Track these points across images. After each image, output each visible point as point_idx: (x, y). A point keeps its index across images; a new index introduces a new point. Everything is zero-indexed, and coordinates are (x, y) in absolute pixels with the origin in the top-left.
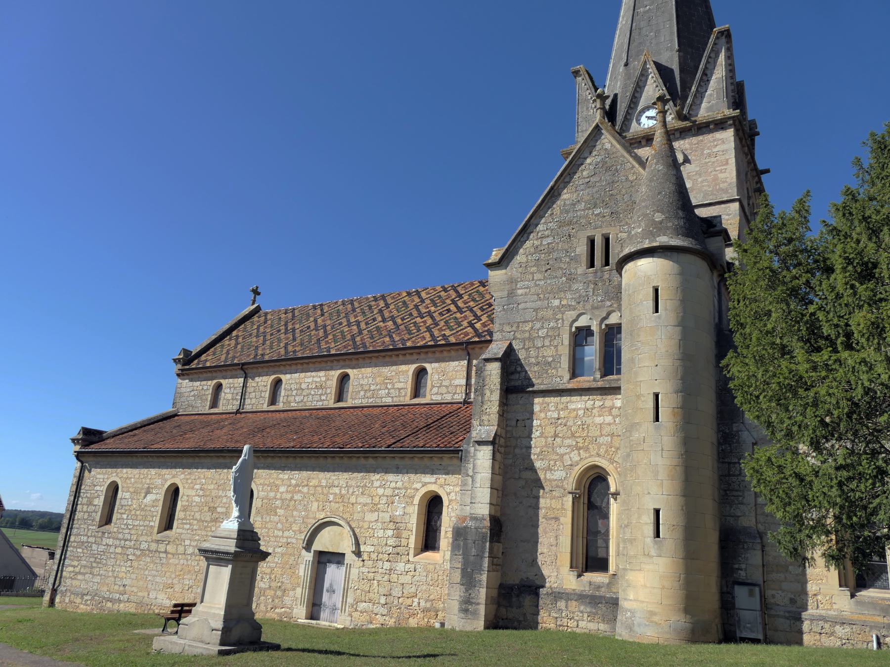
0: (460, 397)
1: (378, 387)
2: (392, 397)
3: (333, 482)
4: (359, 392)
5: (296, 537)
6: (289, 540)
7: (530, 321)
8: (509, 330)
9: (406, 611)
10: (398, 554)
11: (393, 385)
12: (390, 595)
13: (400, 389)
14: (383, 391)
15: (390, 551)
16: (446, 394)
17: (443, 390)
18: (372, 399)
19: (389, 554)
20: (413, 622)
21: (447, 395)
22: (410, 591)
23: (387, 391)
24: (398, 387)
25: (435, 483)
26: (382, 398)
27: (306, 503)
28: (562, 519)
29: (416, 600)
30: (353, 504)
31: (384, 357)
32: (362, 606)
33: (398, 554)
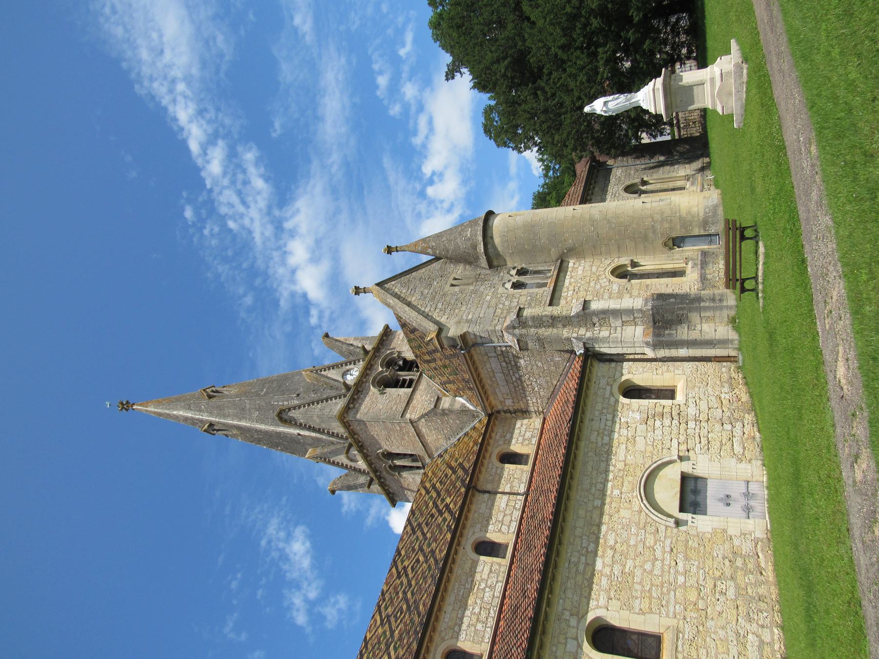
0: (519, 503)
1: (479, 602)
2: (497, 582)
3: (599, 490)
4: (476, 630)
5: (662, 539)
6: (668, 549)
7: (495, 310)
8: (497, 321)
9: (735, 404)
10: (679, 414)
11: (482, 580)
12: (721, 419)
13: (491, 571)
14: (486, 594)
15: (677, 422)
16: (512, 517)
17: (508, 518)
18: (492, 612)
19: (680, 424)
20: (745, 397)
21: (513, 516)
22: (715, 402)
23: (487, 589)
24: (487, 575)
25: (611, 386)
26: (494, 596)
27: (620, 527)
28: (647, 283)
29: (723, 396)
30: (625, 465)
31: (446, 587)
32: (738, 448)
33: (679, 414)
